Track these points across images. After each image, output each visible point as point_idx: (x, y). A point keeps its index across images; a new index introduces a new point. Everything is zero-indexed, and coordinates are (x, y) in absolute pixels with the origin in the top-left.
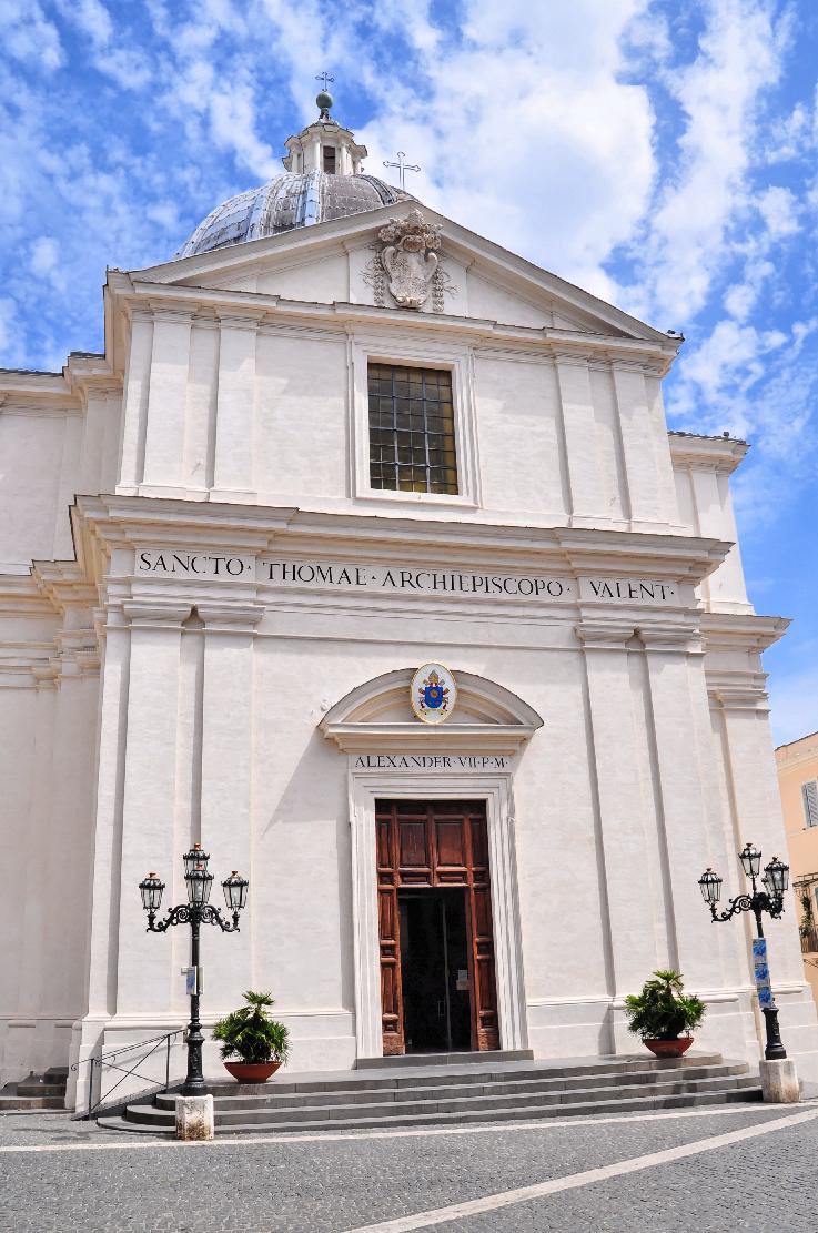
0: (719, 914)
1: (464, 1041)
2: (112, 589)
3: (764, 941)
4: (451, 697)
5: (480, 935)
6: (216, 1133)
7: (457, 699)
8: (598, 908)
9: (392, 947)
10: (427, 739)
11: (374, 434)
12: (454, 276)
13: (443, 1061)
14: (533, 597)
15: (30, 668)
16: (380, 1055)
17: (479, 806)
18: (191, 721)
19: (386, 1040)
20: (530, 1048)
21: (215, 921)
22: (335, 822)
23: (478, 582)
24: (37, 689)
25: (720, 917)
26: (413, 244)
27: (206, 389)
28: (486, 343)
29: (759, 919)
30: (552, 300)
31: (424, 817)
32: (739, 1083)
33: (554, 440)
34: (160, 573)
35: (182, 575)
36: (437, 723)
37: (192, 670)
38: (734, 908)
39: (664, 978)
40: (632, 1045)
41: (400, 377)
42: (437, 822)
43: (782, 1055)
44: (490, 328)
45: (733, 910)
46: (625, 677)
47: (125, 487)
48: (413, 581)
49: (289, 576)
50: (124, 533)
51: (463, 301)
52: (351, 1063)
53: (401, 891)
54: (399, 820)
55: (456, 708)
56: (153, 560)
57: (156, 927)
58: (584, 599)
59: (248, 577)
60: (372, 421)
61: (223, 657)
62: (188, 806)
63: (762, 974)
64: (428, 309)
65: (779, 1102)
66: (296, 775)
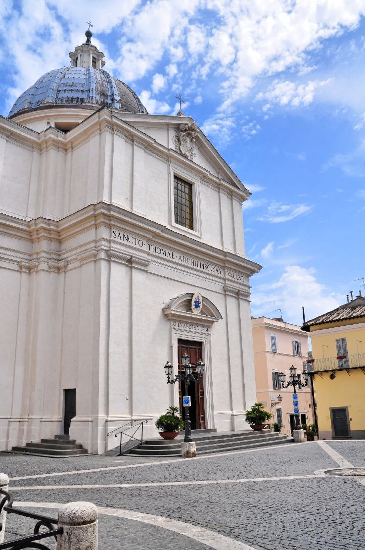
4: (201, 305)
15: (18, 262)
17: (200, 344)
24: (21, 272)
28: (204, 178)
31: (187, 346)
40: (247, 427)
44: (208, 174)
45: (288, 385)
56: (117, 234)
57: (170, 381)
61: (138, 276)
64: (189, 158)
65: (301, 442)
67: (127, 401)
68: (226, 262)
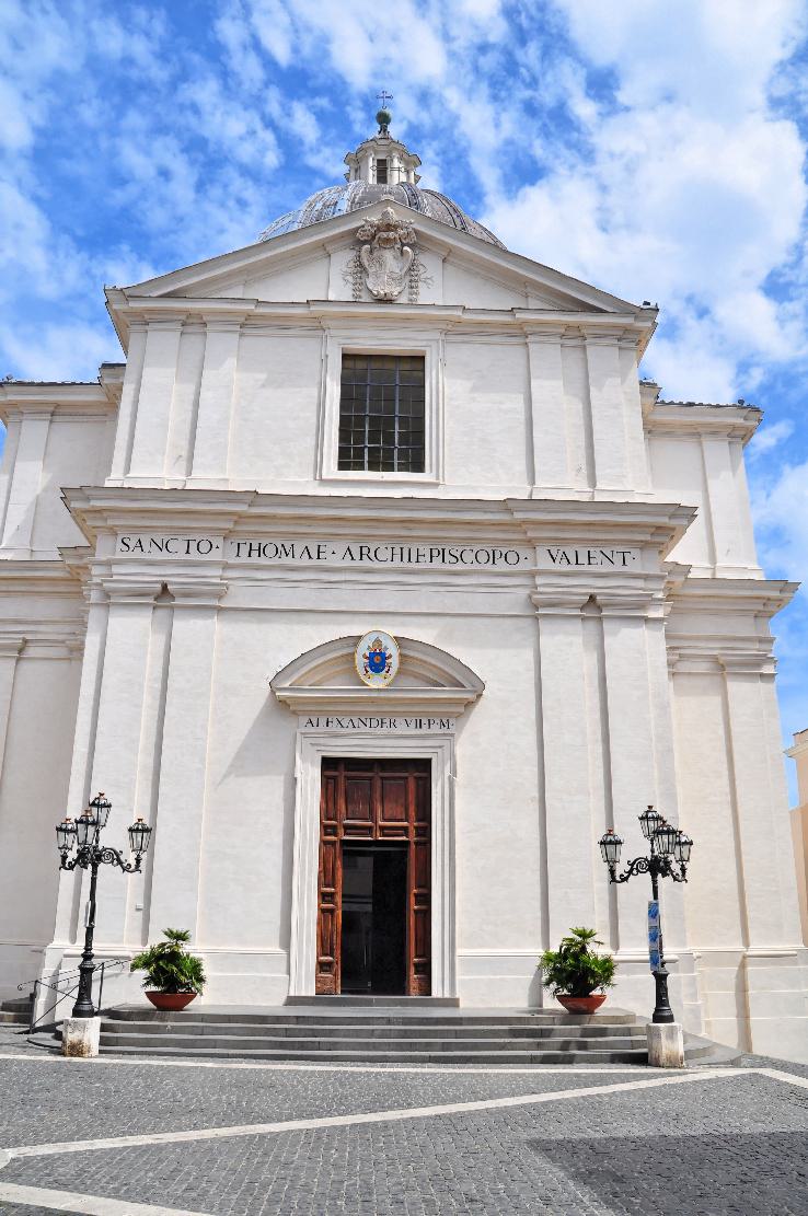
0: (617, 874)
1: (399, 987)
2: (95, 570)
3: (657, 904)
4: (394, 662)
5: (418, 887)
6: (100, 1052)
7: (401, 663)
8: (537, 866)
10: (373, 701)
11: (344, 421)
12: (430, 266)
13: (369, 1003)
14: (489, 567)
15: (63, 642)
16: (312, 993)
17: (425, 765)
18: (158, 686)
20: (457, 996)
21: (115, 862)
22: (282, 778)
23: (435, 553)
25: (618, 879)
26: (387, 240)
27: (191, 388)
28: (458, 328)
29: (655, 882)
30: (527, 283)
31: (370, 774)
32: (633, 1044)
33: (522, 417)
34: (137, 554)
35: (157, 555)
36: (381, 687)
37: (162, 638)
38: (632, 870)
39: (580, 936)
41: (375, 365)
42: (382, 778)
43: (670, 1019)
45: (630, 872)
46: (578, 640)
47: (115, 479)
48: (372, 555)
49: (256, 553)
50: (106, 520)
51: (439, 289)
52: (283, 999)
53: (344, 843)
55: (400, 672)
56: (132, 544)
58: (541, 566)
59: (215, 555)
60: (342, 408)
61: (188, 628)
62: (150, 761)
63: (655, 936)
64: (403, 299)
65: (658, 1065)
66: (250, 733)
67: (140, 914)
68: (524, 527)
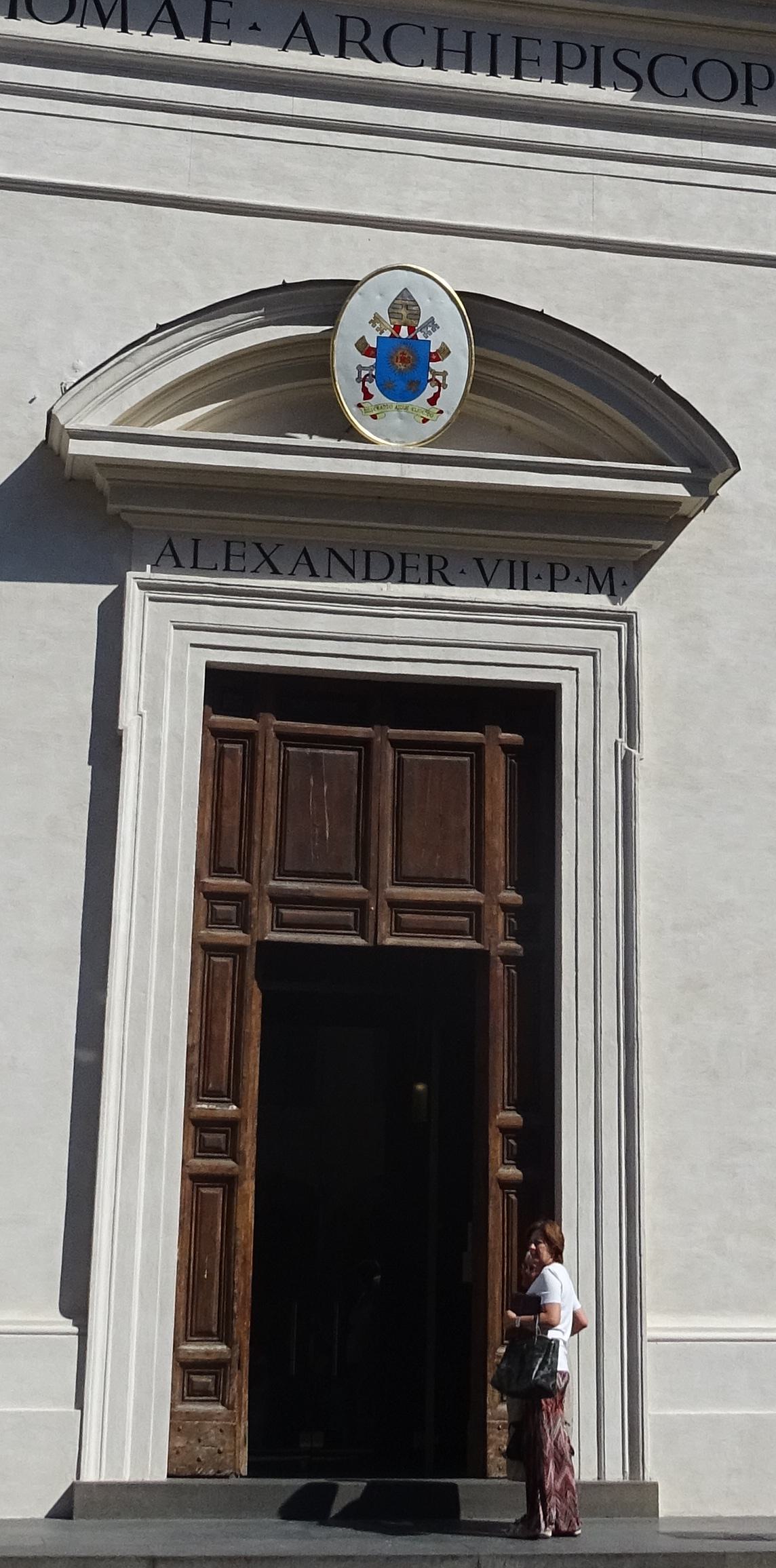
9: (231, 1126)
16: (157, 1472)
19: (178, 1425)
42: (396, 744)
53: (265, 947)
54: (280, 736)
